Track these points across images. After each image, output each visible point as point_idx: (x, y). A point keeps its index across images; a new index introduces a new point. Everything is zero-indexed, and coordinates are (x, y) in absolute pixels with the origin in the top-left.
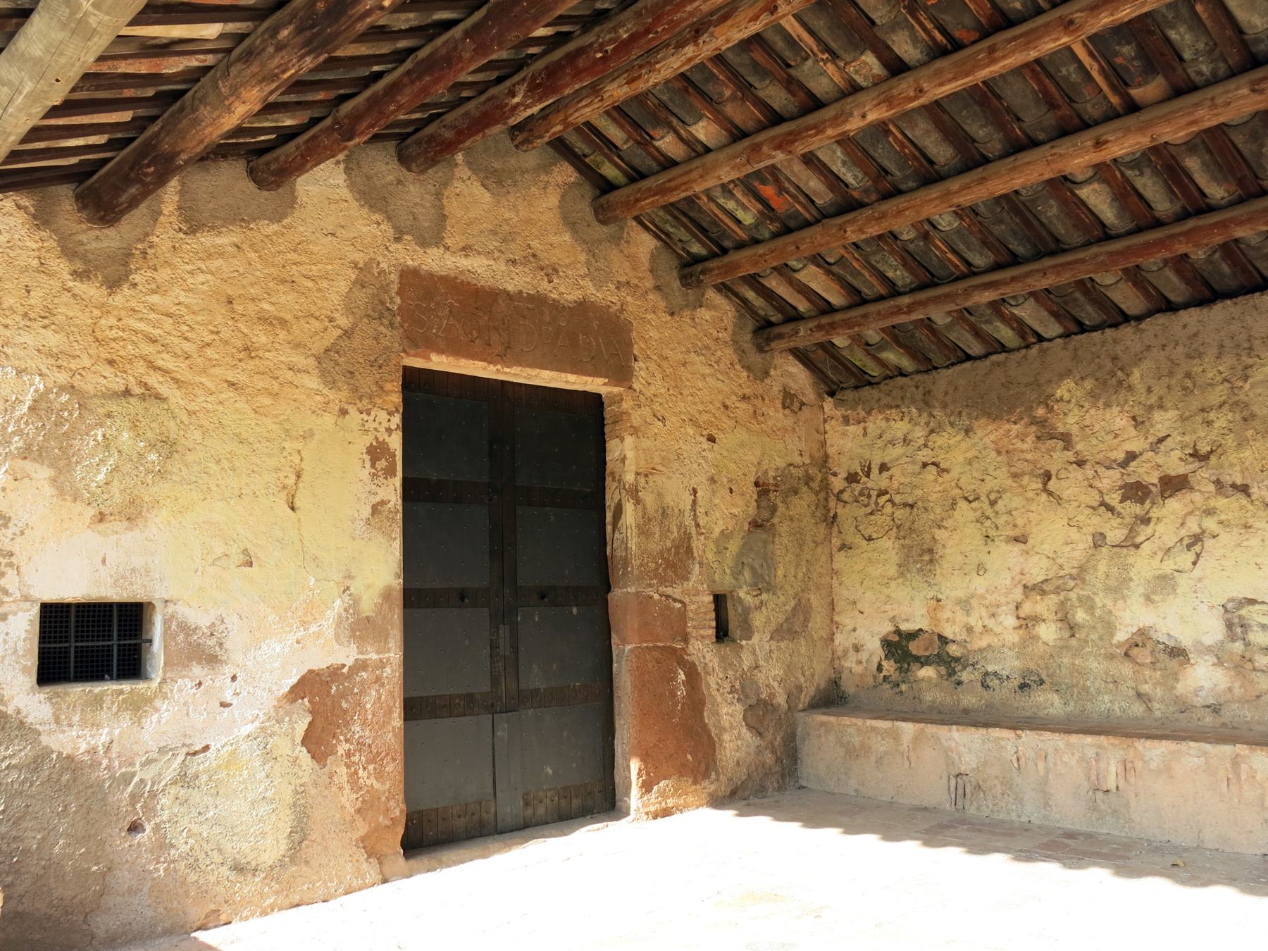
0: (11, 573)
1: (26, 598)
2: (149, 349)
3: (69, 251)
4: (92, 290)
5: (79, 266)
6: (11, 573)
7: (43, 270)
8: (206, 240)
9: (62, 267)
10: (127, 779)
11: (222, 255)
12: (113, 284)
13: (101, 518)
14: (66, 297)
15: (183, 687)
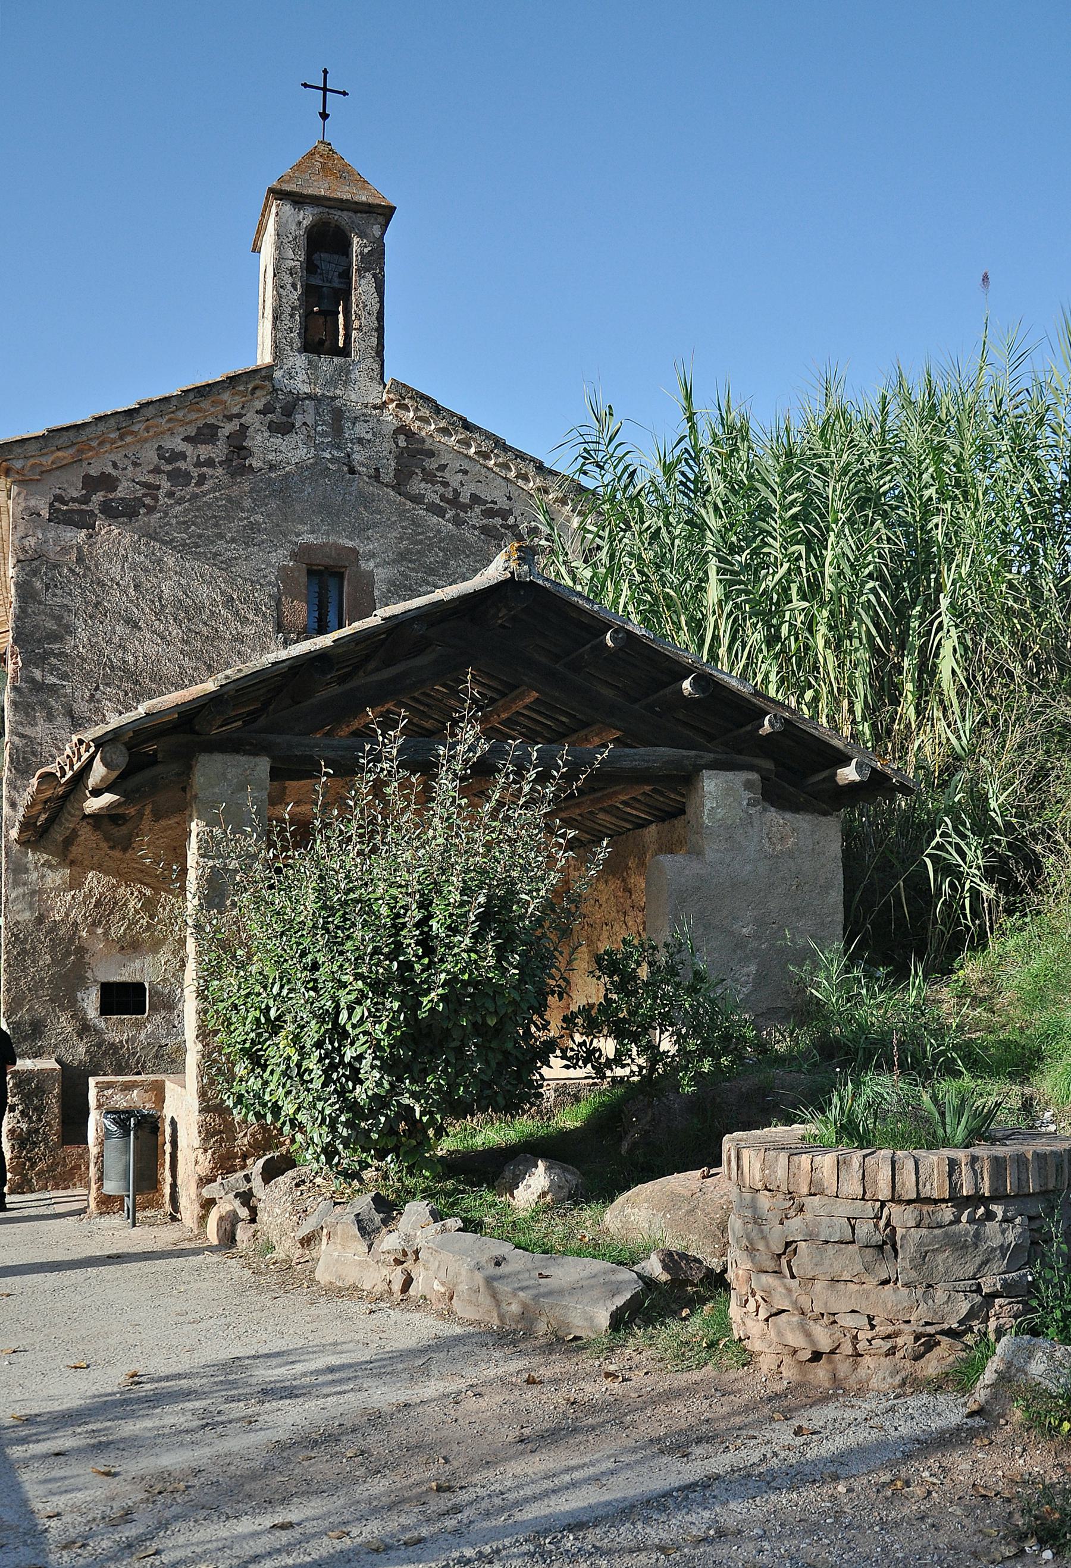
0: (90, 971)
1: (95, 981)
2: (139, 875)
3: (107, 839)
4: (117, 854)
5: (111, 844)
6: (90, 971)
7: (98, 848)
8: (164, 823)
9: (104, 845)
10: (134, 1054)
11: (170, 828)
12: (125, 850)
13: (123, 948)
14: (107, 858)
15: (158, 1018)
